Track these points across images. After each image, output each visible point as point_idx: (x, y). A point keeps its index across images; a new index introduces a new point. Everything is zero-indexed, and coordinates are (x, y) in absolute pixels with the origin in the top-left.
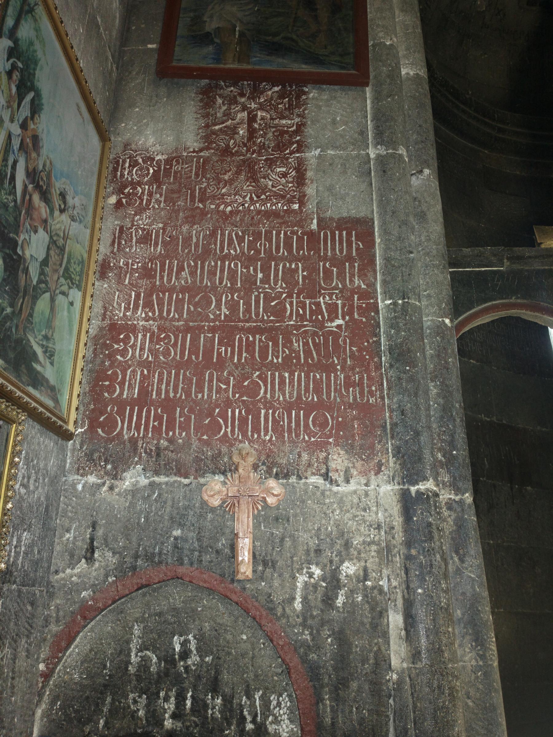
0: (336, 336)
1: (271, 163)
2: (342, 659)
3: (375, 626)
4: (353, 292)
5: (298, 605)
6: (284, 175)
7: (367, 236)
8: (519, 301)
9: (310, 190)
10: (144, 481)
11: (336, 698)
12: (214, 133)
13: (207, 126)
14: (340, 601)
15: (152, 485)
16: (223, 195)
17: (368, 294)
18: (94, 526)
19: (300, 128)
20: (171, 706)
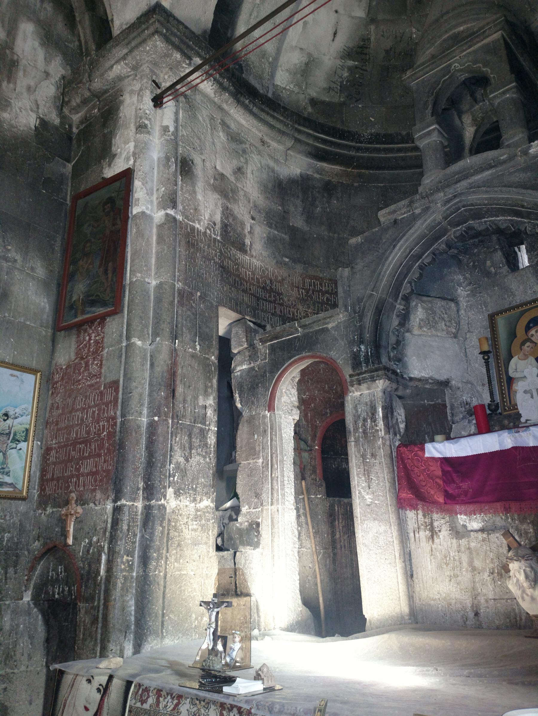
0: (103, 439)
1: (94, 359)
2: (89, 573)
3: (98, 560)
4: (110, 418)
5: (81, 554)
6: (97, 364)
7: (117, 390)
8: (307, 354)
9: (103, 371)
10: (51, 511)
11: (86, 586)
12: (80, 350)
13: (78, 346)
14: (91, 551)
15: (53, 512)
16: (79, 380)
17: (114, 418)
18: (39, 528)
19: (103, 338)
20: (57, 591)
